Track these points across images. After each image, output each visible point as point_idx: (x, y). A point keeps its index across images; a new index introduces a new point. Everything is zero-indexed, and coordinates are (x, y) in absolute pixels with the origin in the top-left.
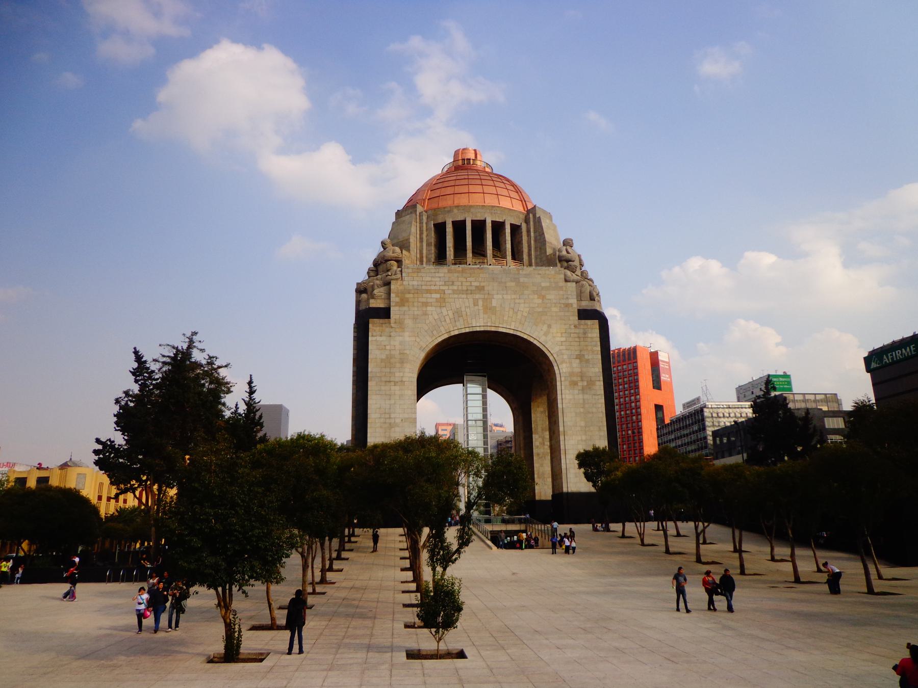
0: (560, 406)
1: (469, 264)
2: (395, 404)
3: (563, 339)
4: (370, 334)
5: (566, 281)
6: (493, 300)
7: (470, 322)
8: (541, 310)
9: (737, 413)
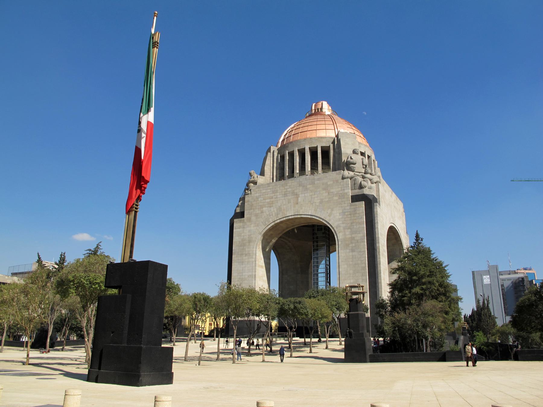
2: (245, 267)
3: (341, 217)
5: (343, 178)
6: (299, 198)
7: (285, 213)
8: (327, 200)
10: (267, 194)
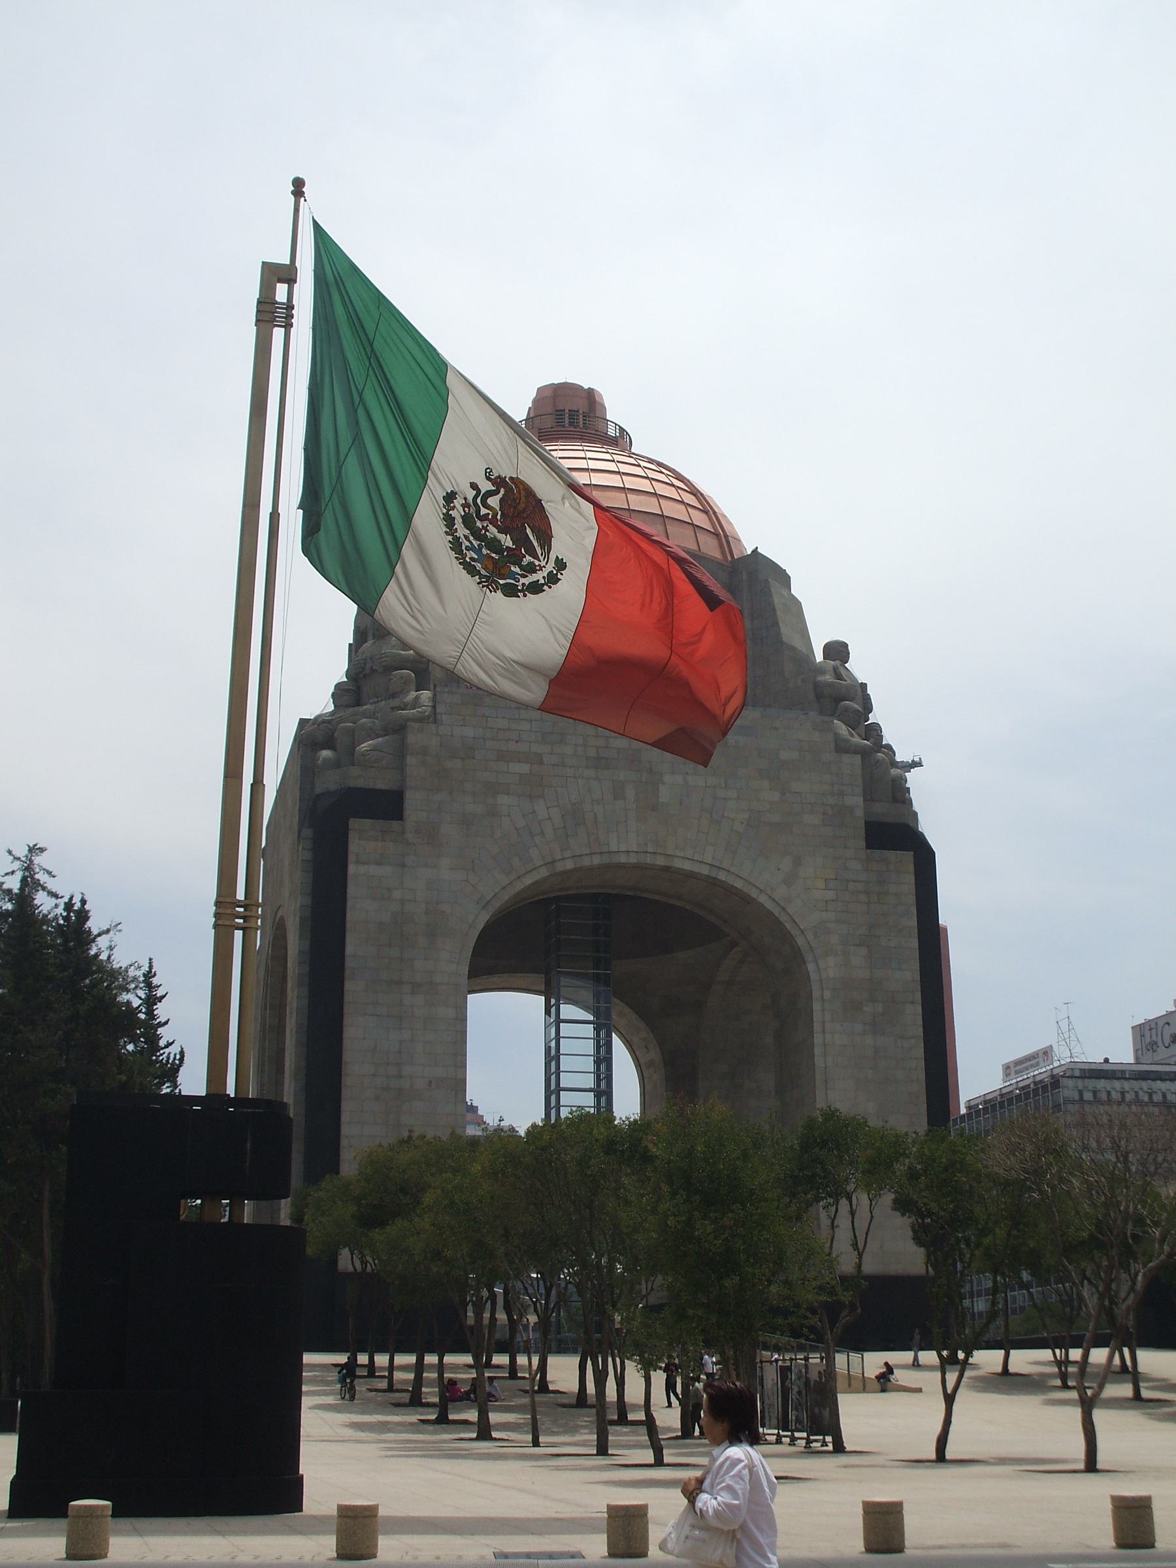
0: (819, 1061)
3: (830, 895)
4: (351, 858)
9: (1141, 1093)
10: (517, 742)
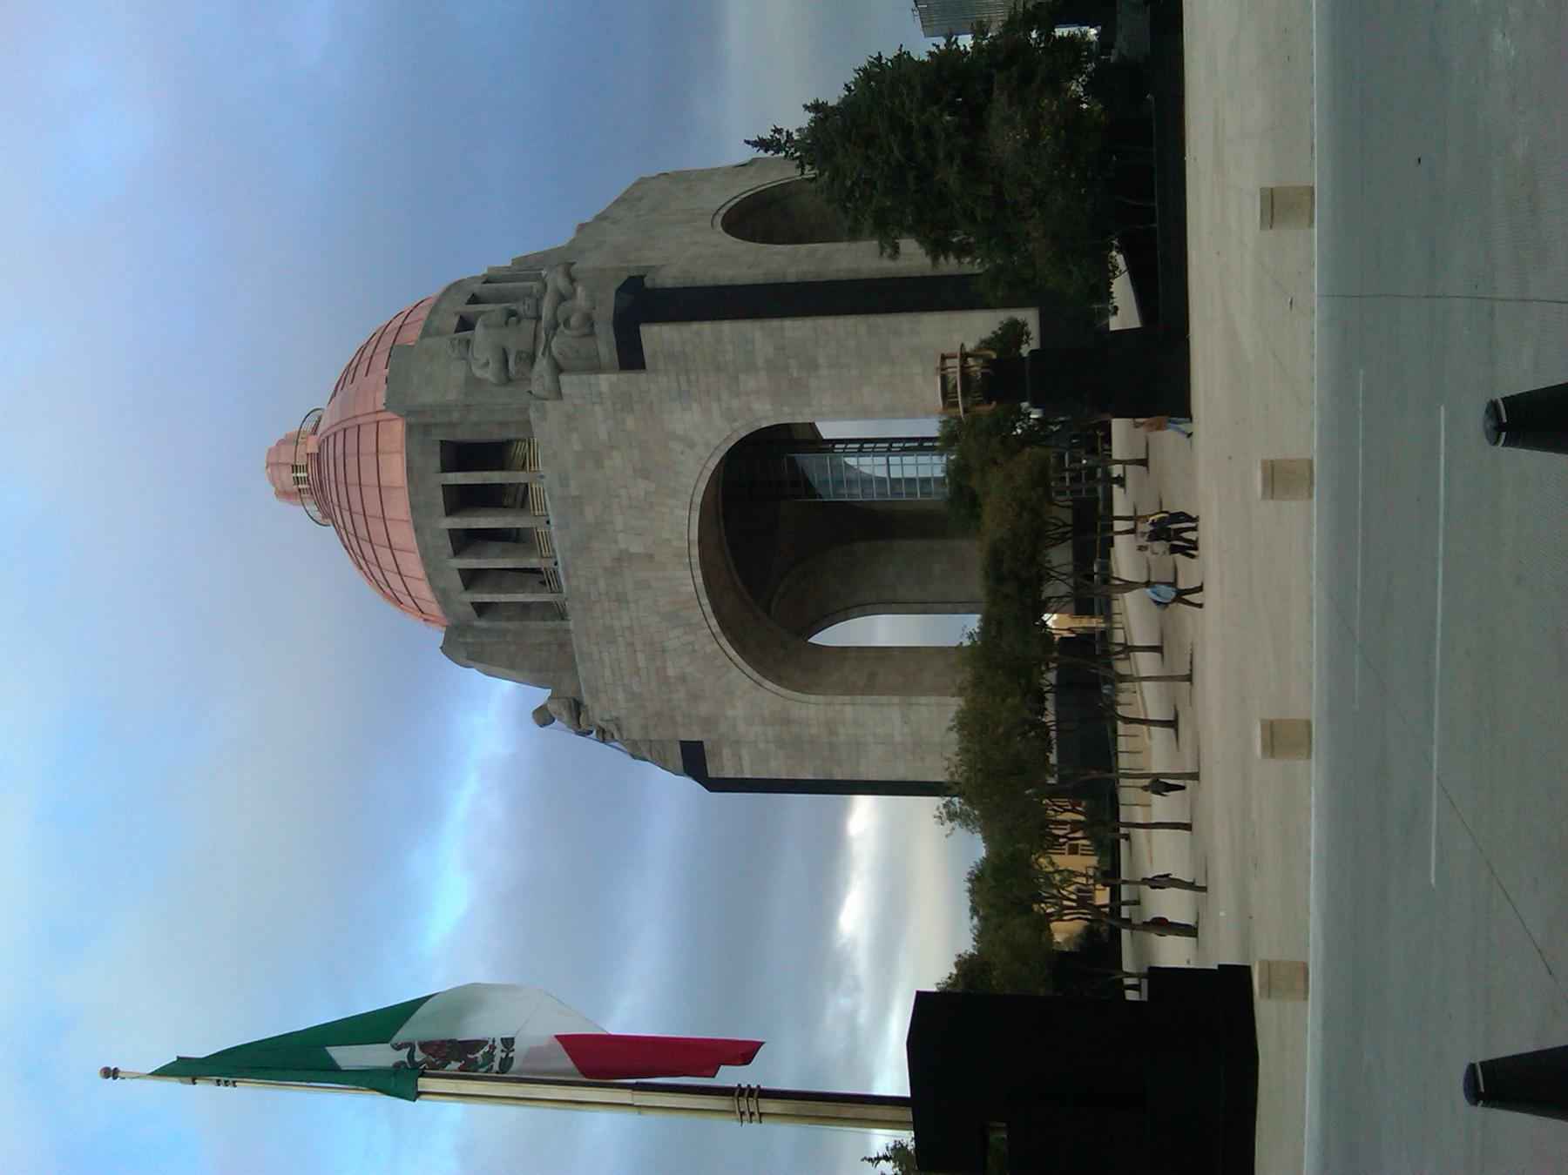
1: (556, 564)
2: (874, 735)
3: (695, 405)
5: (559, 395)
10: (620, 662)
